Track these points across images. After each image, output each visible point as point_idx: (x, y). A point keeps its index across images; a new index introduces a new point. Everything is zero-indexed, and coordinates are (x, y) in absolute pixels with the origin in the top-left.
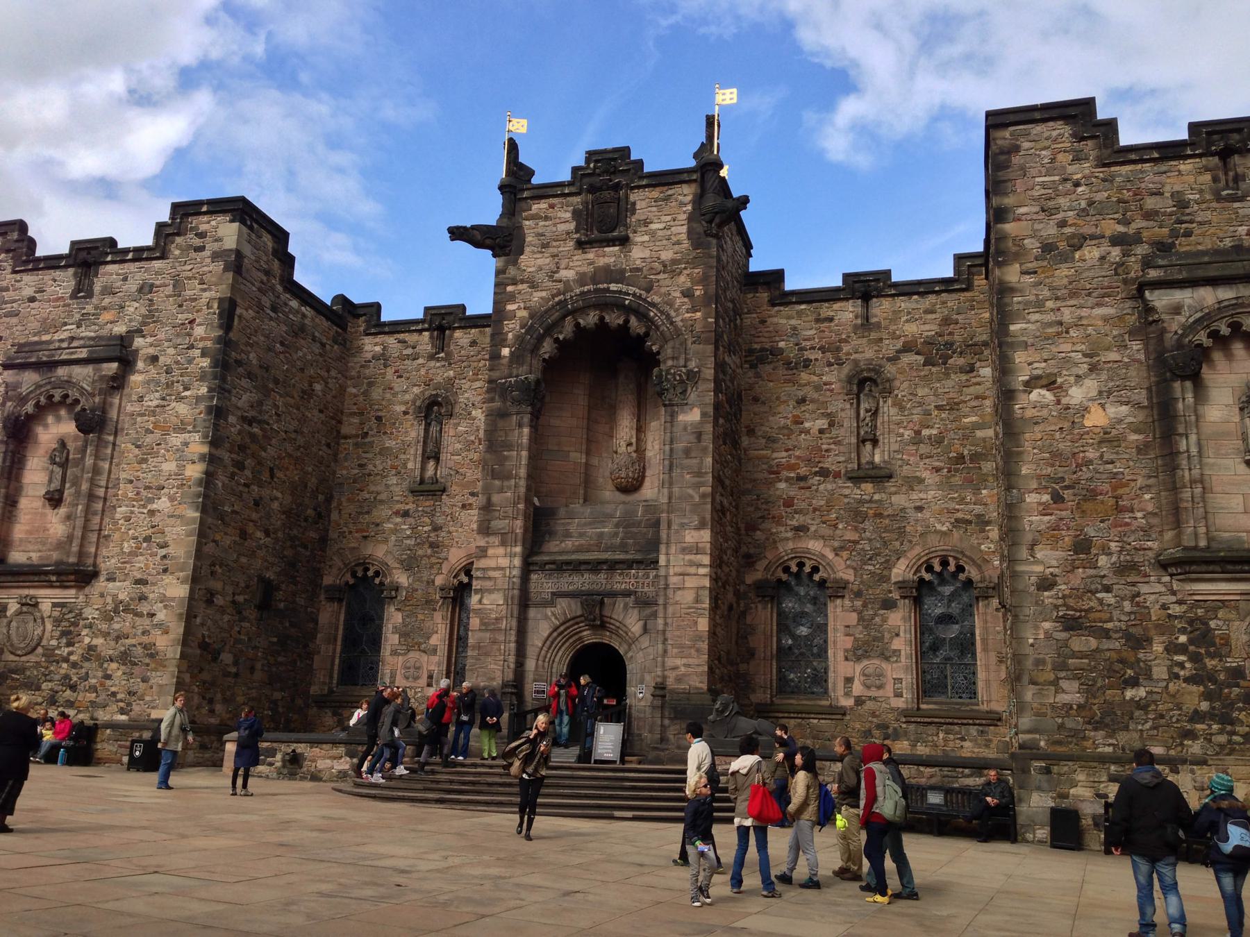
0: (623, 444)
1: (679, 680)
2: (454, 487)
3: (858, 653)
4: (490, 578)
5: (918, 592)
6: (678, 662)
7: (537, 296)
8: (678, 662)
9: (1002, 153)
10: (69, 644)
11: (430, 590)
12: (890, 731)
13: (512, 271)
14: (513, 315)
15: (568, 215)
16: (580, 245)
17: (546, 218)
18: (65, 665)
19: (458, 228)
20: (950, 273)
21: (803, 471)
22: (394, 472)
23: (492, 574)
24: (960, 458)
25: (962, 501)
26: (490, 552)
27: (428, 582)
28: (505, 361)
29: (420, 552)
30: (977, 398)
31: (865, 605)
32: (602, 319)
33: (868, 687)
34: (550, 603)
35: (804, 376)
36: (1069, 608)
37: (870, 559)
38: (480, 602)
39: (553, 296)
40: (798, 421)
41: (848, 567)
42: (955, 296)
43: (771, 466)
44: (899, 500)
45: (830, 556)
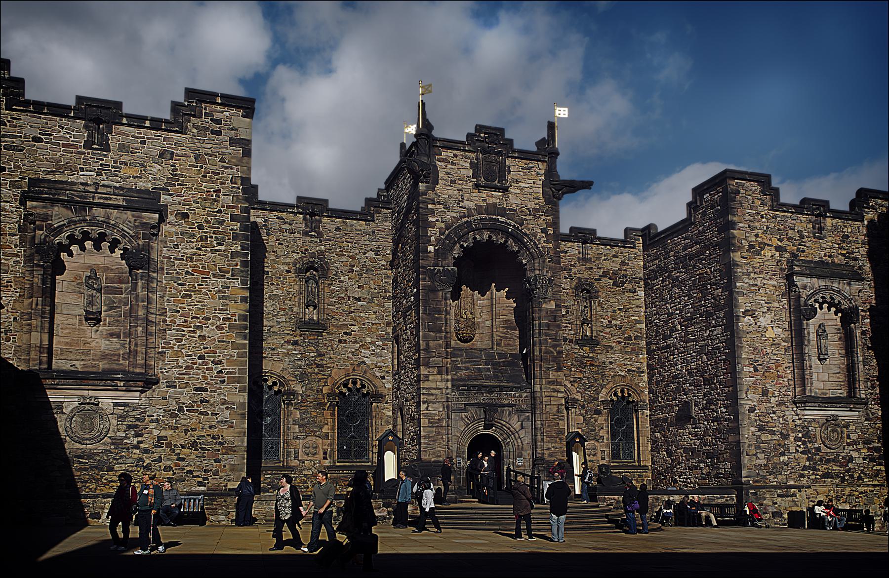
4: (432, 394)
10: (137, 435)
18: (137, 451)
23: (433, 392)
24: (630, 338)
26: (431, 378)
29: (310, 370)
36: (761, 421)
44: (602, 357)
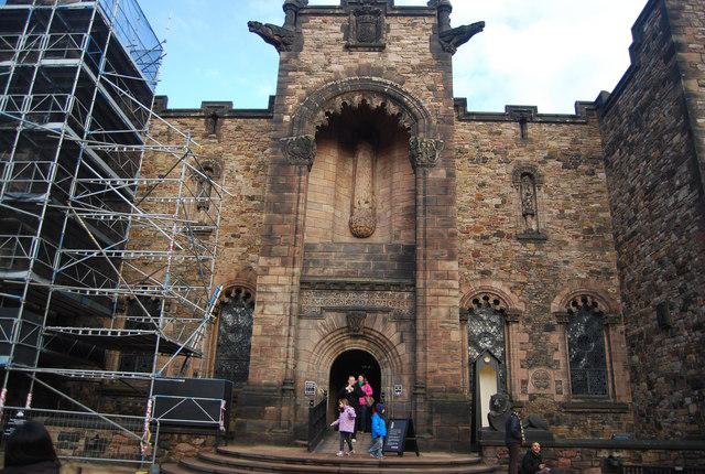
0: (362, 202)
1: (437, 381)
3: (530, 363)
5: (567, 319)
6: (435, 365)
7: (312, 81)
8: (435, 365)
9: (674, 9)
12: (554, 418)
13: (293, 62)
14: (292, 93)
15: (338, 28)
16: (347, 48)
17: (321, 29)
19: (256, 23)
20: (573, 112)
21: (485, 232)
23: (274, 289)
24: (590, 230)
25: (594, 258)
26: (272, 271)
32: (364, 101)
33: (539, 388)
34: (319, 316)
35: (483, 169)
39: (326, 82)
40: (480, 198)
41: (520, 301)
42: (578, 126)
43: (462, 228)
45: (508, 293)
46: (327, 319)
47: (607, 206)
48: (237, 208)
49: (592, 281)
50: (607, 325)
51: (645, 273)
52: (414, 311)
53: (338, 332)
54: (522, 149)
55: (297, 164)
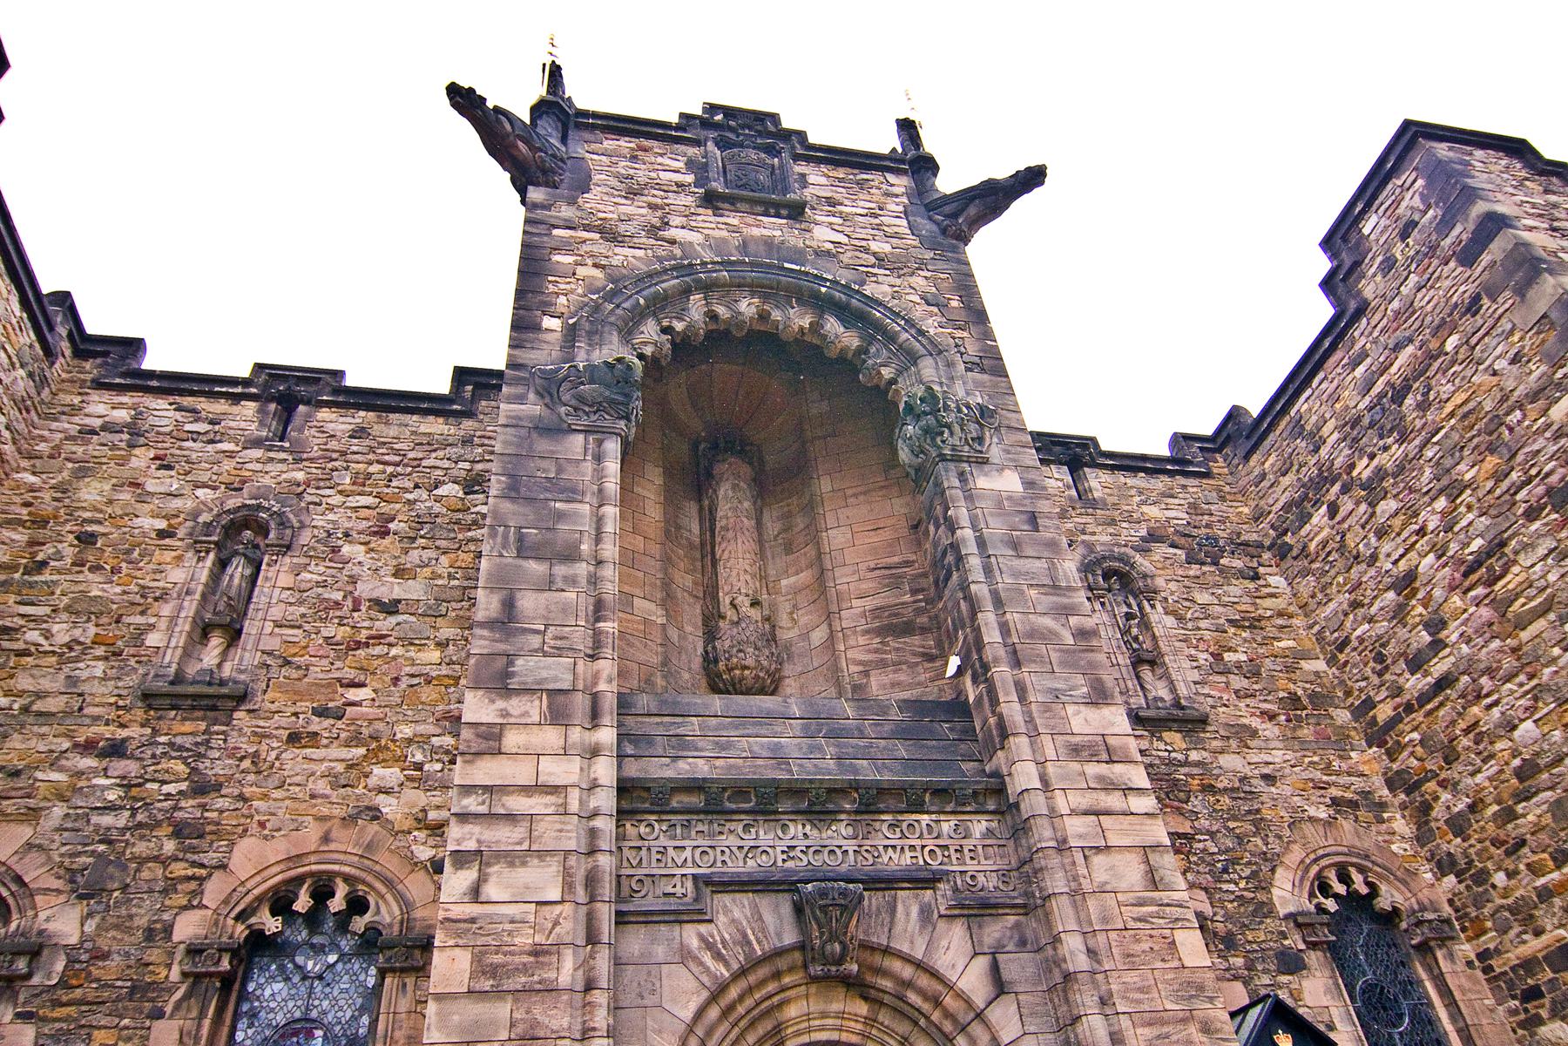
2: (270, 695)
4: (511, 818)
11: (154, 955)
16: (711, 200)
22: (100, 651)
25: (1328, 769)
26: (512, 740)
27: (150, 934)
28: (556, 337)
29: (141, 848)
30: (1280, 614)
31: (1250, 967)
34: (696, 914)
37: (1225, 870)
38: (475, 893)
46: (722, 919)
47: (1309, 644)
48: (342, 633)
49: (1347, 825)
50: (1424, 949)
51: (1527, 771)
52: (1026, 869)
53: (762, 972)
54: (1089, 519)
55: (586, 432)
